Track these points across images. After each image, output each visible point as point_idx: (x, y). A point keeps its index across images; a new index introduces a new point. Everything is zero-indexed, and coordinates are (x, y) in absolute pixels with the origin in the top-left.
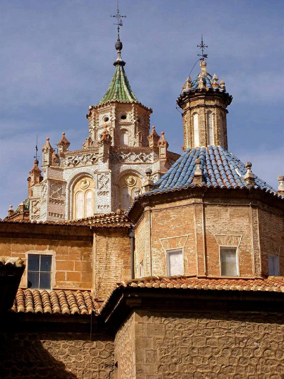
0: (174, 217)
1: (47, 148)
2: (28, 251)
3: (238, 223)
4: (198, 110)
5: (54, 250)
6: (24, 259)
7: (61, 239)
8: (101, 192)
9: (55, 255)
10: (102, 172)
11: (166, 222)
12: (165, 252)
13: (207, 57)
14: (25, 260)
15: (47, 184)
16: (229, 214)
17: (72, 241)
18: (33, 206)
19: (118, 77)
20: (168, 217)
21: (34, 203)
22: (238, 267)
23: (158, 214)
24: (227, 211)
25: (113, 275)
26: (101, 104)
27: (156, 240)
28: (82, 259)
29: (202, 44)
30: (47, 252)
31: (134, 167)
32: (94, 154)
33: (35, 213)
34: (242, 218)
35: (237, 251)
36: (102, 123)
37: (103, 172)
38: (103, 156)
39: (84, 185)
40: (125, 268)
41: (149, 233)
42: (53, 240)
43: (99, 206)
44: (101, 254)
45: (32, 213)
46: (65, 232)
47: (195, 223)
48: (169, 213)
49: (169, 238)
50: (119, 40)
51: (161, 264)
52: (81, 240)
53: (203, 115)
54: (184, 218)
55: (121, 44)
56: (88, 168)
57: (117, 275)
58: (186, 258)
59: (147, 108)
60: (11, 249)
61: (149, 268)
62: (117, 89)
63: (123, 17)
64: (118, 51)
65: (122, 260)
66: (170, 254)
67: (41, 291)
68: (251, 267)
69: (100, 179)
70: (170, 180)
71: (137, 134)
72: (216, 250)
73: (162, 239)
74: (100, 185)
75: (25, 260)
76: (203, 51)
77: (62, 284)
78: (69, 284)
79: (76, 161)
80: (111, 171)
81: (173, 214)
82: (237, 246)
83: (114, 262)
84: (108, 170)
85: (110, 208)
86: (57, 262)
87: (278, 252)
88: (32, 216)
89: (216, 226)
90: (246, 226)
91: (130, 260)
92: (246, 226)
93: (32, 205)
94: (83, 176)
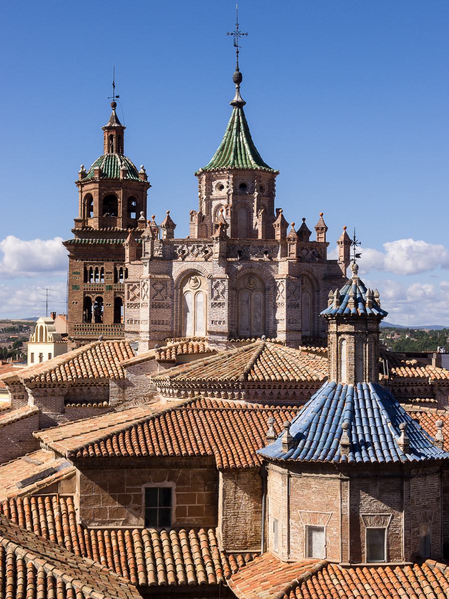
0: (315, 487)
1: (148, 236)
2: (144, 484)
3: (388, 500)
4: (347, 337)
5: (173, 481)
6: (140, 493)
7: (182, 468)
8: (215, 303)
9: (175, 487)
10: (217, 278)
11: (306, 492)
12: (305, 527)
13: (360, 257)
14: (141, 495)
15: (148, 282)
16: (378, 489)
17: (194, 469)
18: (128, 291)
19: (235, 126)
21: (131, 287)
23: (297, 480)
24: (376, 486)
26: (215, 168)
27: (294, 511)
28: (206, 490)
29: (354, 240)
32: (207, 246)
33: (132, 300)
34: (393, 493)
36: (216, 193)
37: (219, 278)
38: (220, 256)
39: (194, 285)
40: (256, 512)
41: (287, 501)
42: (173, 469)
43: (213, 321)
44: (228, 498)
45: (128, 299)
46: (186, 463)
47: (340, 501)
48: (310, 482)
49: (310, 511)
50: (238, 70)
52: (205, 468)
53: (353, 345)
54: (327, 492)
55: (240, 75)
56: (199, 264)
57: (247, 521)
58: (328, 539)
59: (273, 171)
60: (126, 483)
61: (286, 542)
62: (234, 144)
63: (243, 34)
64: (237, 86)
65: (253, 504)
66: (311, 530)
69: (216, 287)
70: (310, 434)
71: (260, 214)
73: (301, 511)
74: (215, 294)
75: (142, 494)
76: (355, 249)
77: (184, 520)
78: (191, 520)
79: (184, 252)
80: (228, 277)
81: (313, 483)
82: (386, 527)
83: (243, 506)
84: (225, 276)
85: (226, 325)
86: (177, 495)
87: (431, 520)
88: (128, 304)
90: (399, 502)
92: (397, 502)
93: (128, 289)
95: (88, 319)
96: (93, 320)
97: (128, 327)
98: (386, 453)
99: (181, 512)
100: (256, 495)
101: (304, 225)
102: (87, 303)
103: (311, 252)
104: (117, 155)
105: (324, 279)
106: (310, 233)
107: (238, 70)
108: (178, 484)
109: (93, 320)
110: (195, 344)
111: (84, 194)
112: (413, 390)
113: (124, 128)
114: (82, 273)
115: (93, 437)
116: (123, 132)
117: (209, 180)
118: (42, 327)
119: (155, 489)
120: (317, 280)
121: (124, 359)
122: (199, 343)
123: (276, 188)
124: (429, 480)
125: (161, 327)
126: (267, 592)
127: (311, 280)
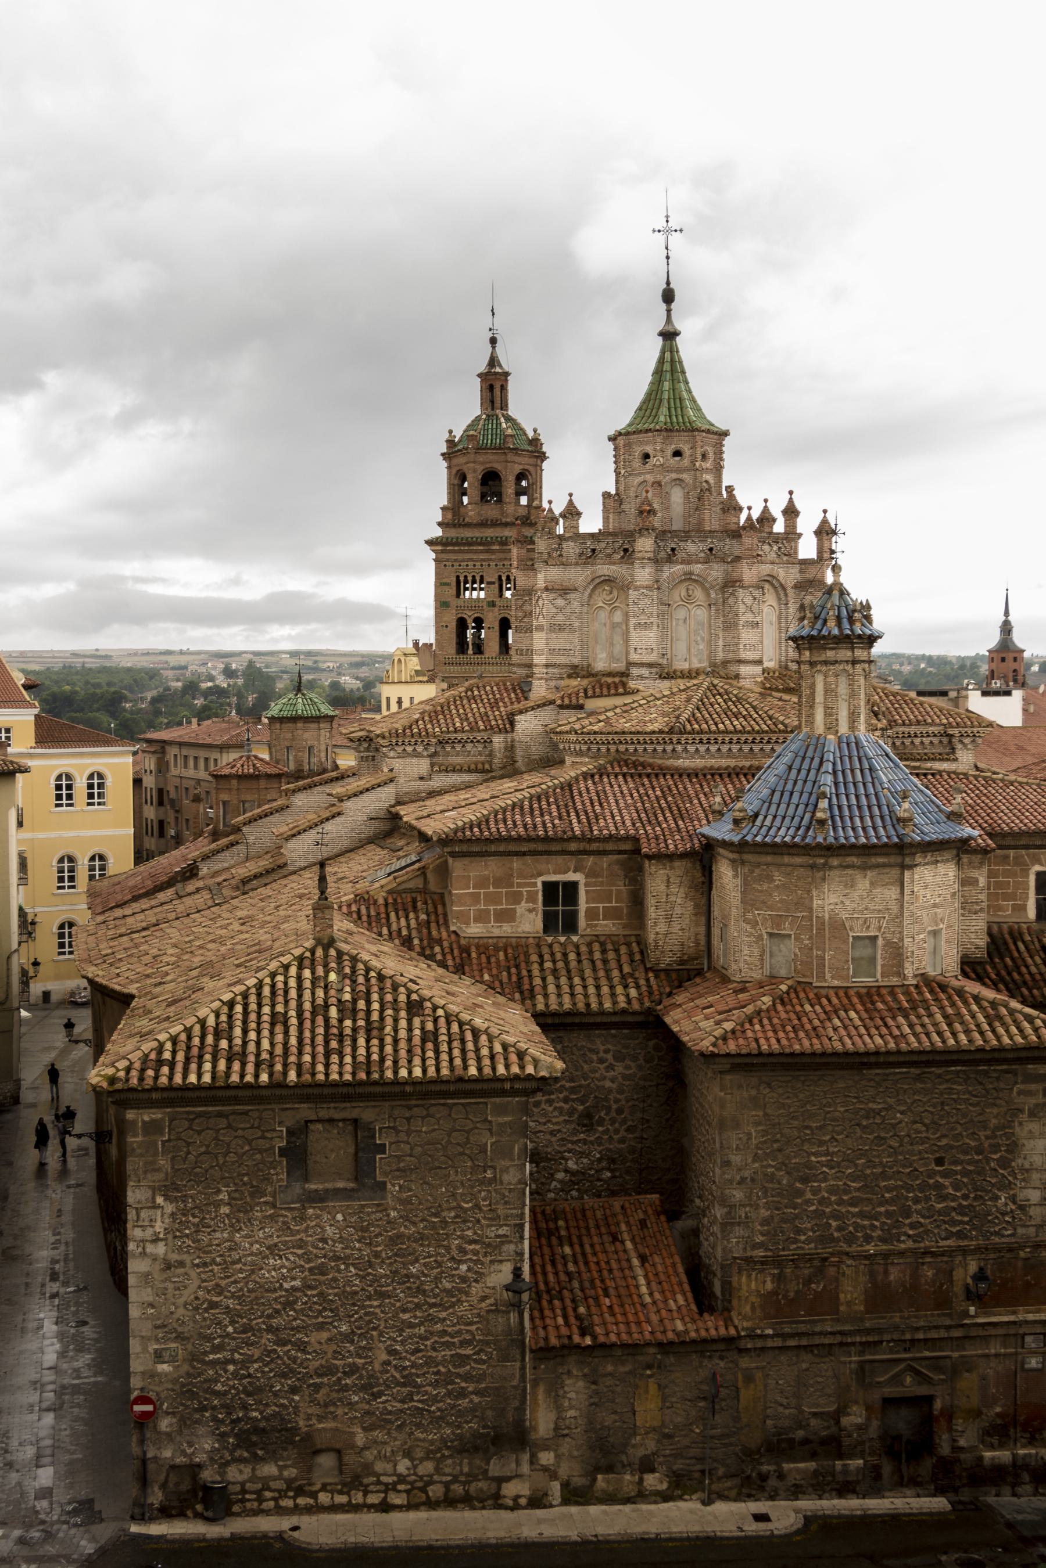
11: (765, 886)
20: (770, 879)
22: (879, 968)
25: (676, 927)
30: (571, 877)
31: (697, 568)
35: (880, 942)
40: (696, 915)
50: (668, 283)
51: (756, 952)
53: (831, 679)
67: (562, 939)
68: (901, 965)
72: (846, 941)
77: (596, 925)
79: (593, 550)
86: (587, 892)
89: (847, 903)
91: (704, 901)
94: (608, 581)
95: (462, 646)
96: (470, 651)
97: (515, 658)
98: (882, 832)
99: (591, 914)
100: (697, 891)
101: (766, 509)
102: (462, 625)
103: (775, 548)
104: (498, 411)
105: (795, 587)
106: (774, 520)
107: (668, 283)
108: (587, 877)
109: (470, 651)
110: (609, 680)
111: (454, 471)
112: (922, 743)
113: (506, 374)
114: (454, 584)
115: (470, 815)
116: (506, 381)
117: (628, 446)
118: (400, 661)
119: (555, 884)
120: (784, 589)
121: (512, 703)
122: (617, 680)
123: (725, 456)
124: (942, 868)
125: (562, 660)
126: (711, 1022)
127: (775, 588)
